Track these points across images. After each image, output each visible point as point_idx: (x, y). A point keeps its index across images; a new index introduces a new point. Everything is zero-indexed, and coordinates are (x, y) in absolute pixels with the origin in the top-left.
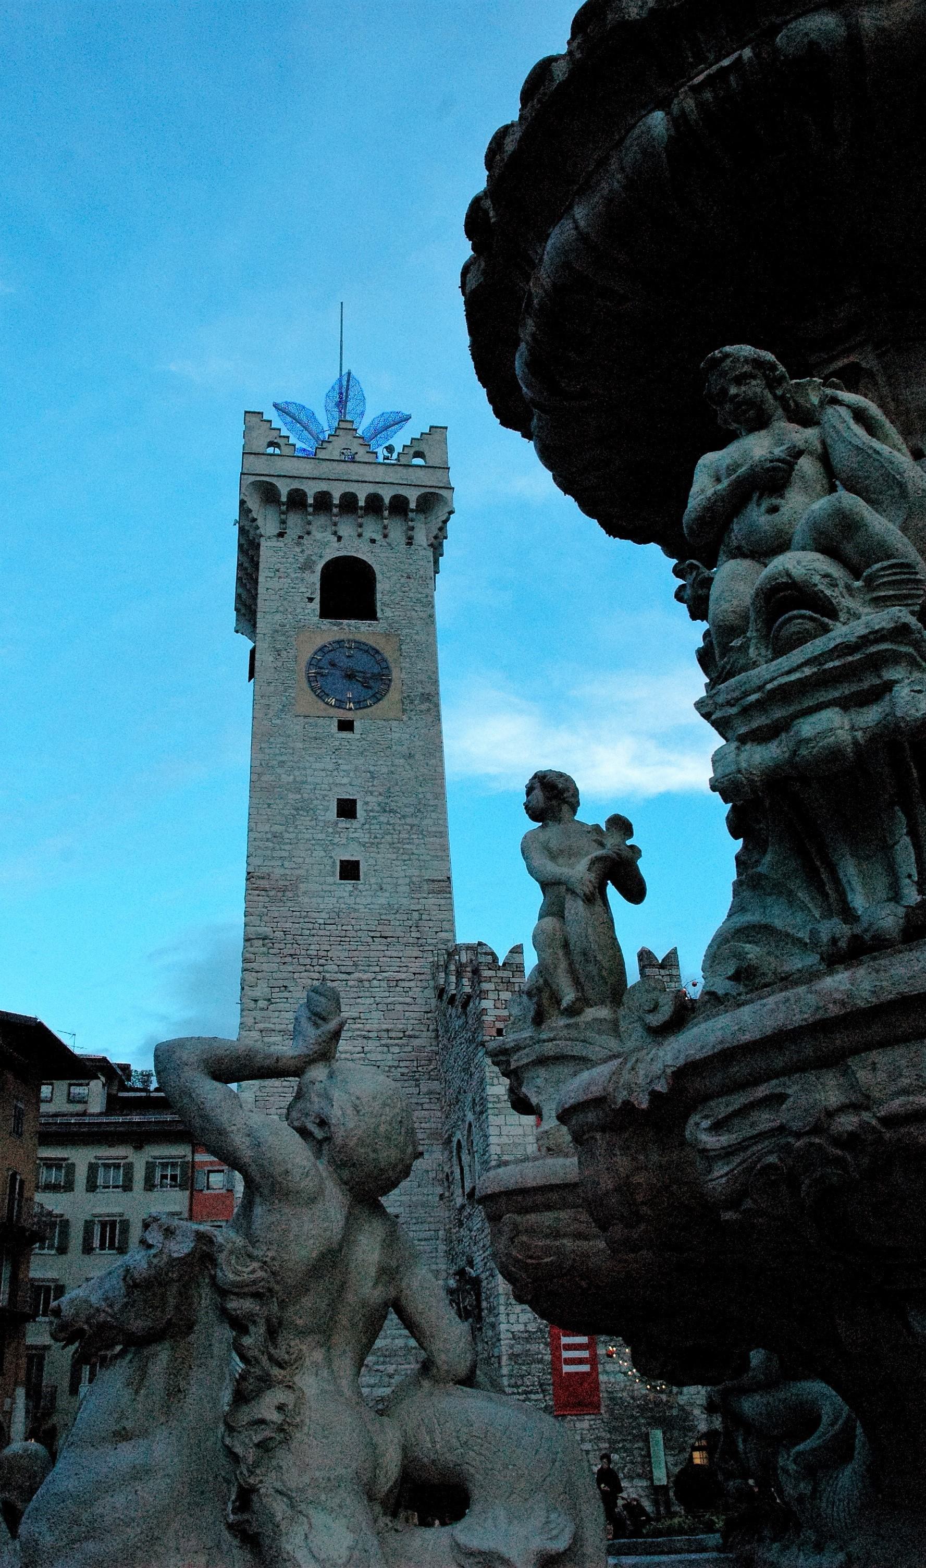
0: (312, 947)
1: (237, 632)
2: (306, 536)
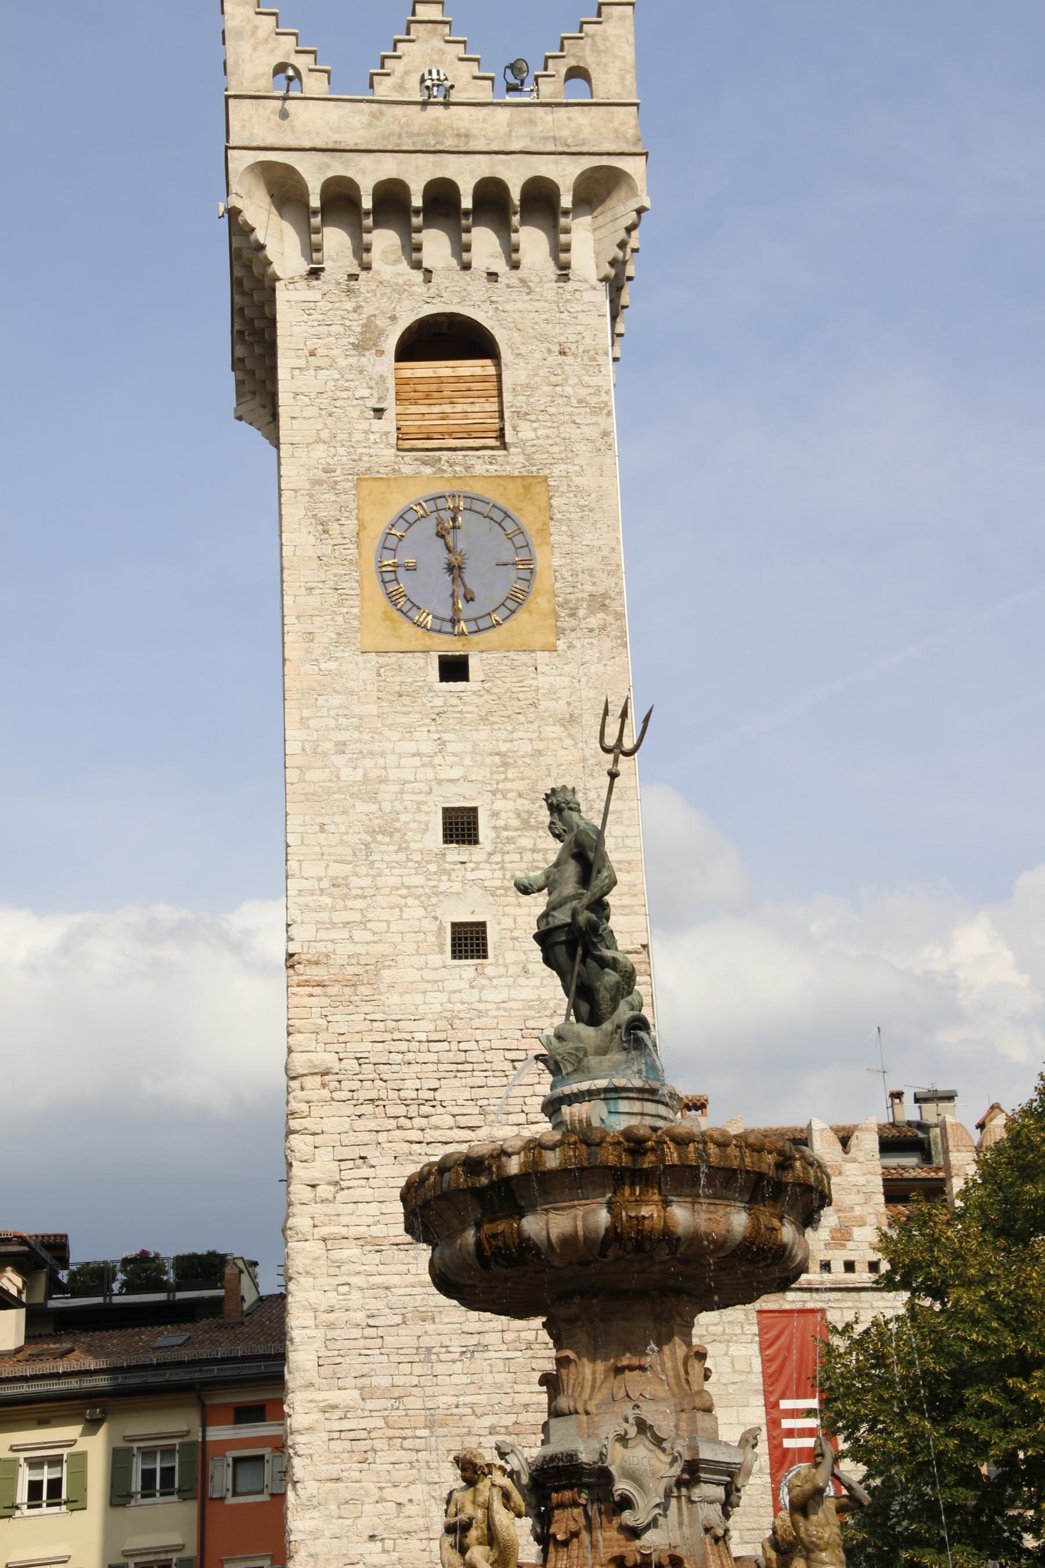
0: (408, 1084)
1: (240, 418)
2: (363, 275)
